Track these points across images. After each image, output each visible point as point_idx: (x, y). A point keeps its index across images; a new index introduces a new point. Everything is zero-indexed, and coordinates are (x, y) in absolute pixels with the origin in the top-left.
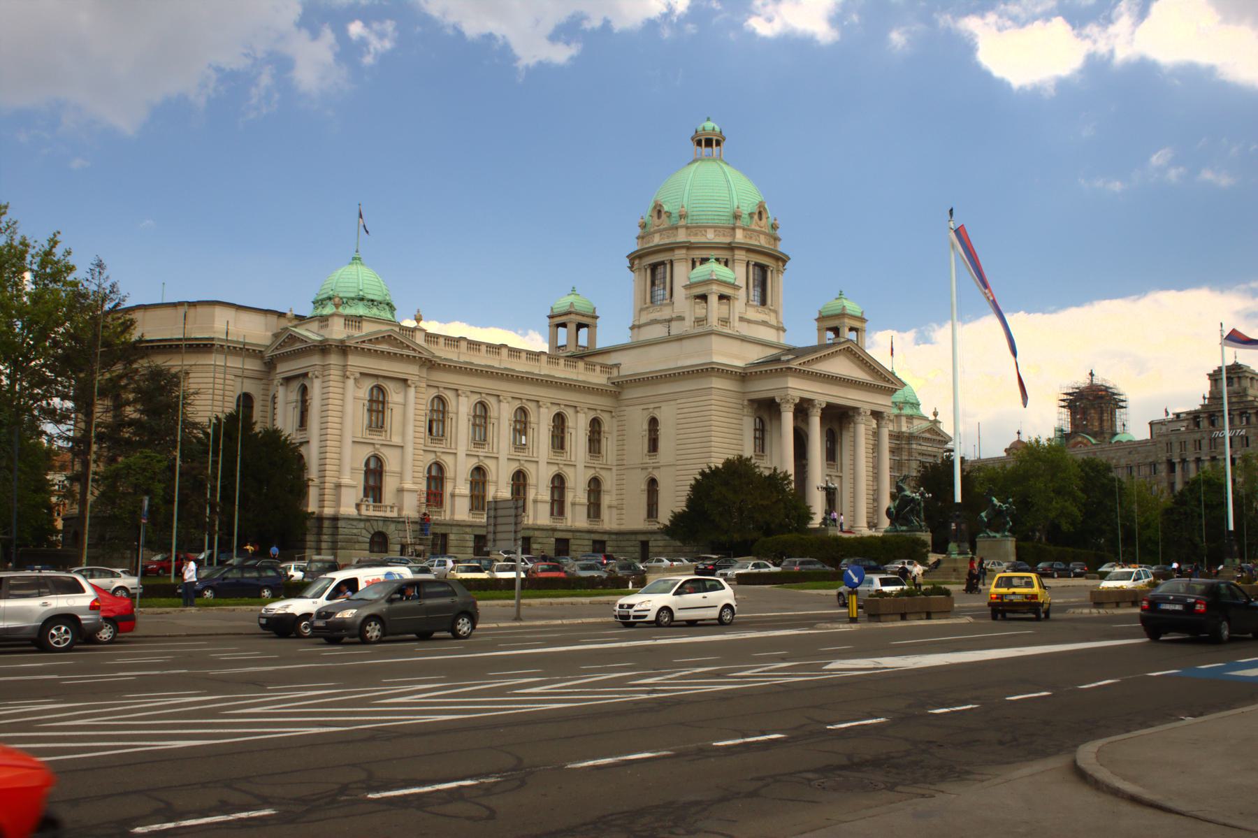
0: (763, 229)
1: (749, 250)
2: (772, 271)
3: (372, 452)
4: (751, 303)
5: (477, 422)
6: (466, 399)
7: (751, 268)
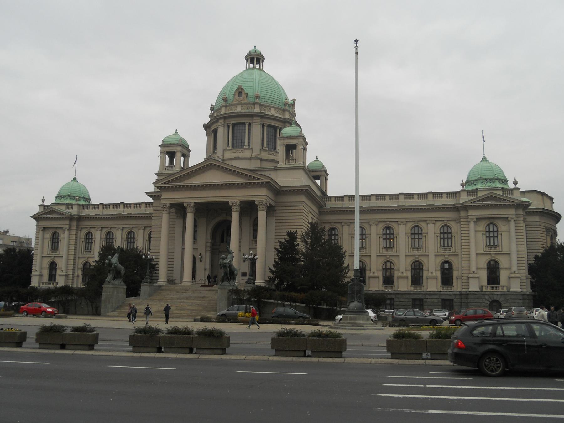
0: (243, 102)
1: (226, 117)
2: (250, 125)
3: (490, 258)
4: (228, 148)
5: (111, 240)
6: (348, 227)
7: (231, 127)
